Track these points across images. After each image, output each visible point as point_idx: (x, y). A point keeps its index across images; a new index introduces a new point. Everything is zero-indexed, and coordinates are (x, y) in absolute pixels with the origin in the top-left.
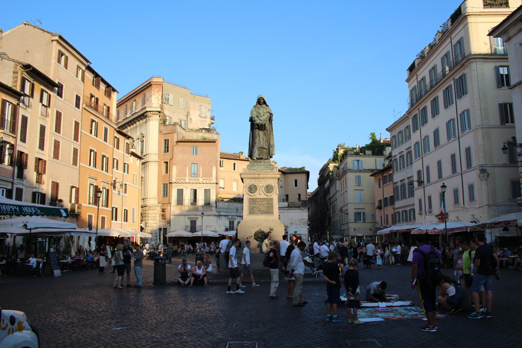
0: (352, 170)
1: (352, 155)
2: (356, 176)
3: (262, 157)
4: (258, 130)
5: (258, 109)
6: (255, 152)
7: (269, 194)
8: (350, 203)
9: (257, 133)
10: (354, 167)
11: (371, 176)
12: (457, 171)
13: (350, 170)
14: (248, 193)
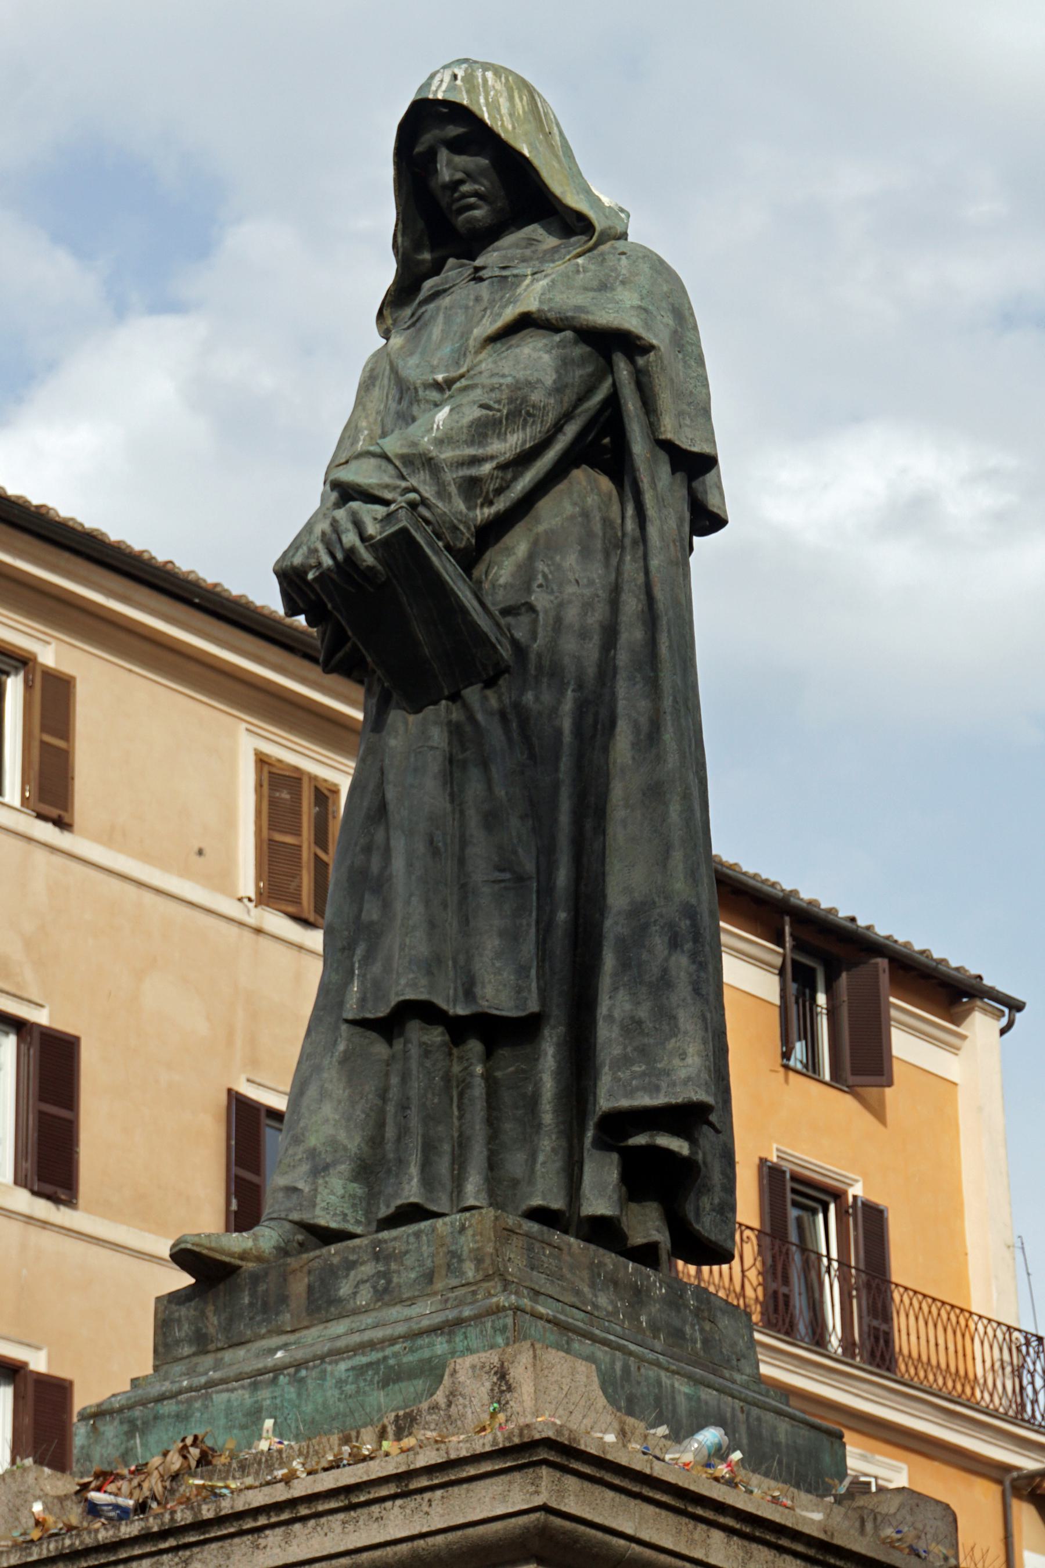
3: (412, 1192)
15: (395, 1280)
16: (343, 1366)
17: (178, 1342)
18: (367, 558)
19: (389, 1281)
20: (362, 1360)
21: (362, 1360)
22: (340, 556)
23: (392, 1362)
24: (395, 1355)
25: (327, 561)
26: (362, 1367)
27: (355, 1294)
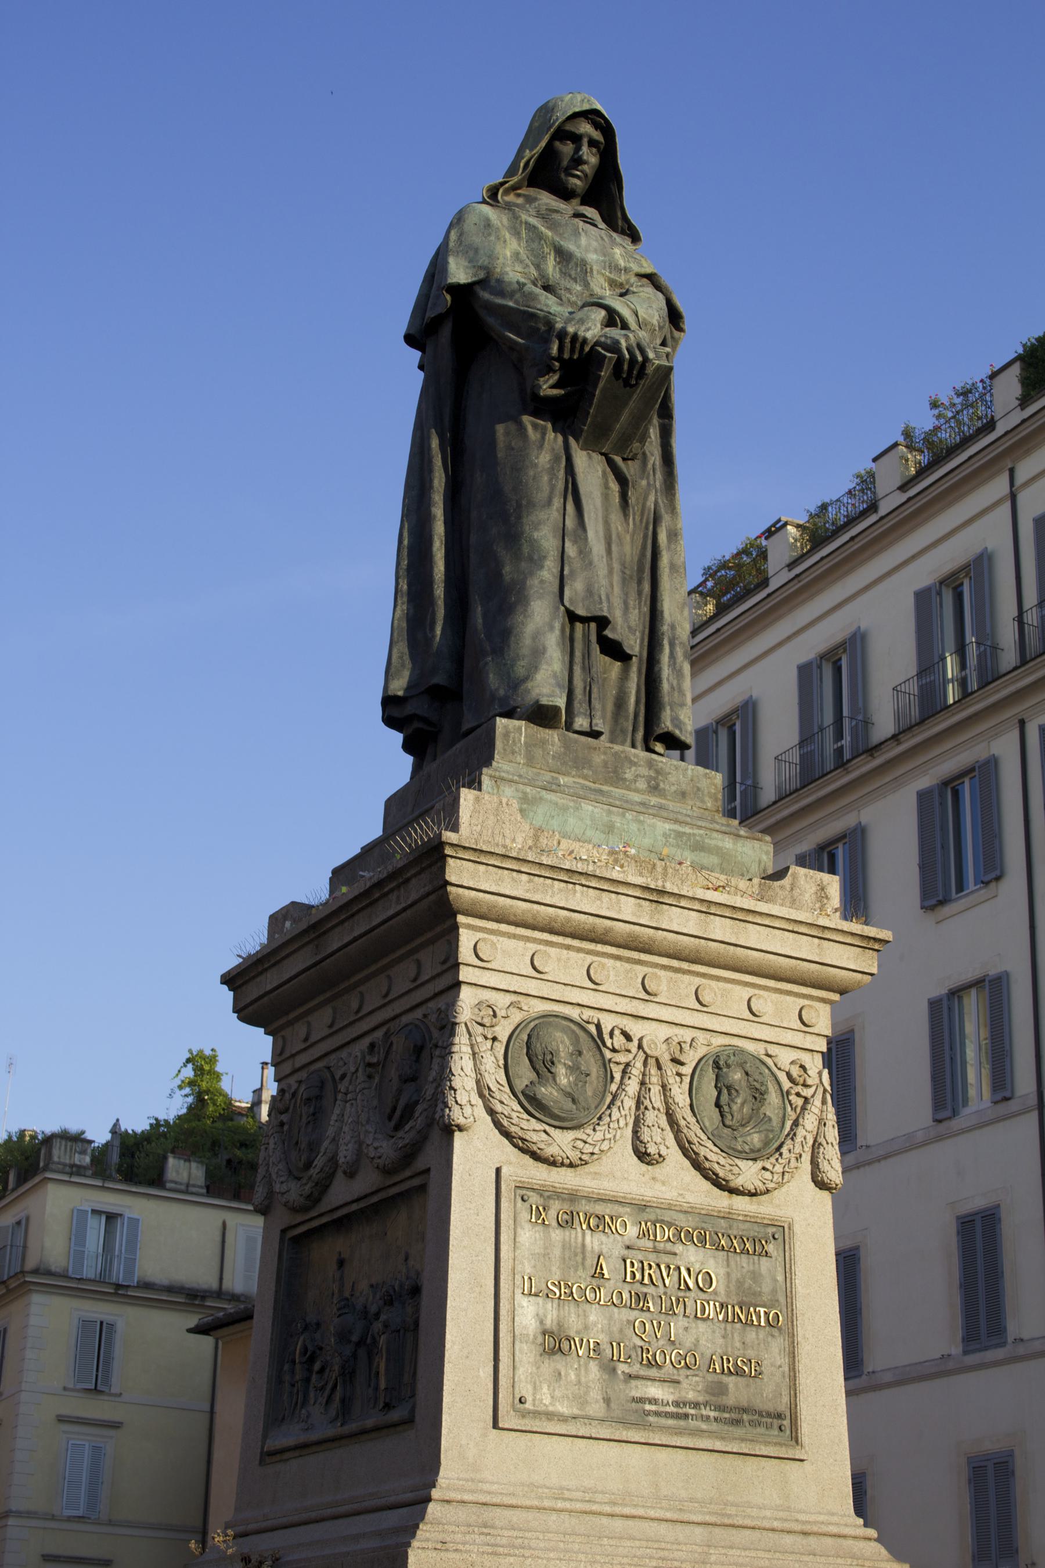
0: (64, 1276)
1: (76, 1170)
2: (85, 1324)
4: (554, 439)
5: (545, 215)
6: (538, 653)
7: (748, 1174)
8: (19, 1514)
9: (544, 459)
10: (80, 1256)
11: (200, 1330)
12: (1013, 1329)
13: (49, 1273)
14: (510, 1107)
15: (662, 785)
16: (667, 826)
17: (513, 752)
18: (650, 370)
19: (658, 785)
20: (681, 829)
21: (676, 827)
22: (640, 359)
23: (697, 838)
24: (701, 836)
25: (627, 356)
26: (679, 832)
27: (635, 781)
